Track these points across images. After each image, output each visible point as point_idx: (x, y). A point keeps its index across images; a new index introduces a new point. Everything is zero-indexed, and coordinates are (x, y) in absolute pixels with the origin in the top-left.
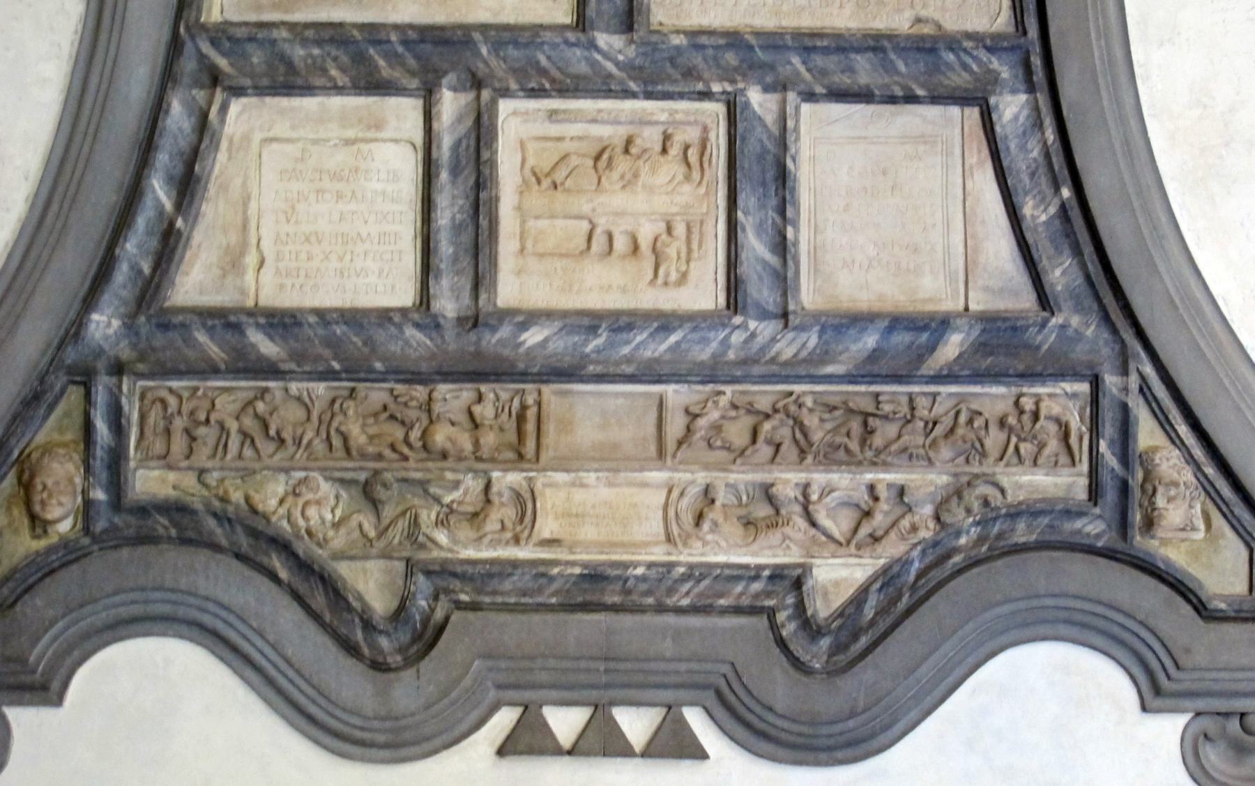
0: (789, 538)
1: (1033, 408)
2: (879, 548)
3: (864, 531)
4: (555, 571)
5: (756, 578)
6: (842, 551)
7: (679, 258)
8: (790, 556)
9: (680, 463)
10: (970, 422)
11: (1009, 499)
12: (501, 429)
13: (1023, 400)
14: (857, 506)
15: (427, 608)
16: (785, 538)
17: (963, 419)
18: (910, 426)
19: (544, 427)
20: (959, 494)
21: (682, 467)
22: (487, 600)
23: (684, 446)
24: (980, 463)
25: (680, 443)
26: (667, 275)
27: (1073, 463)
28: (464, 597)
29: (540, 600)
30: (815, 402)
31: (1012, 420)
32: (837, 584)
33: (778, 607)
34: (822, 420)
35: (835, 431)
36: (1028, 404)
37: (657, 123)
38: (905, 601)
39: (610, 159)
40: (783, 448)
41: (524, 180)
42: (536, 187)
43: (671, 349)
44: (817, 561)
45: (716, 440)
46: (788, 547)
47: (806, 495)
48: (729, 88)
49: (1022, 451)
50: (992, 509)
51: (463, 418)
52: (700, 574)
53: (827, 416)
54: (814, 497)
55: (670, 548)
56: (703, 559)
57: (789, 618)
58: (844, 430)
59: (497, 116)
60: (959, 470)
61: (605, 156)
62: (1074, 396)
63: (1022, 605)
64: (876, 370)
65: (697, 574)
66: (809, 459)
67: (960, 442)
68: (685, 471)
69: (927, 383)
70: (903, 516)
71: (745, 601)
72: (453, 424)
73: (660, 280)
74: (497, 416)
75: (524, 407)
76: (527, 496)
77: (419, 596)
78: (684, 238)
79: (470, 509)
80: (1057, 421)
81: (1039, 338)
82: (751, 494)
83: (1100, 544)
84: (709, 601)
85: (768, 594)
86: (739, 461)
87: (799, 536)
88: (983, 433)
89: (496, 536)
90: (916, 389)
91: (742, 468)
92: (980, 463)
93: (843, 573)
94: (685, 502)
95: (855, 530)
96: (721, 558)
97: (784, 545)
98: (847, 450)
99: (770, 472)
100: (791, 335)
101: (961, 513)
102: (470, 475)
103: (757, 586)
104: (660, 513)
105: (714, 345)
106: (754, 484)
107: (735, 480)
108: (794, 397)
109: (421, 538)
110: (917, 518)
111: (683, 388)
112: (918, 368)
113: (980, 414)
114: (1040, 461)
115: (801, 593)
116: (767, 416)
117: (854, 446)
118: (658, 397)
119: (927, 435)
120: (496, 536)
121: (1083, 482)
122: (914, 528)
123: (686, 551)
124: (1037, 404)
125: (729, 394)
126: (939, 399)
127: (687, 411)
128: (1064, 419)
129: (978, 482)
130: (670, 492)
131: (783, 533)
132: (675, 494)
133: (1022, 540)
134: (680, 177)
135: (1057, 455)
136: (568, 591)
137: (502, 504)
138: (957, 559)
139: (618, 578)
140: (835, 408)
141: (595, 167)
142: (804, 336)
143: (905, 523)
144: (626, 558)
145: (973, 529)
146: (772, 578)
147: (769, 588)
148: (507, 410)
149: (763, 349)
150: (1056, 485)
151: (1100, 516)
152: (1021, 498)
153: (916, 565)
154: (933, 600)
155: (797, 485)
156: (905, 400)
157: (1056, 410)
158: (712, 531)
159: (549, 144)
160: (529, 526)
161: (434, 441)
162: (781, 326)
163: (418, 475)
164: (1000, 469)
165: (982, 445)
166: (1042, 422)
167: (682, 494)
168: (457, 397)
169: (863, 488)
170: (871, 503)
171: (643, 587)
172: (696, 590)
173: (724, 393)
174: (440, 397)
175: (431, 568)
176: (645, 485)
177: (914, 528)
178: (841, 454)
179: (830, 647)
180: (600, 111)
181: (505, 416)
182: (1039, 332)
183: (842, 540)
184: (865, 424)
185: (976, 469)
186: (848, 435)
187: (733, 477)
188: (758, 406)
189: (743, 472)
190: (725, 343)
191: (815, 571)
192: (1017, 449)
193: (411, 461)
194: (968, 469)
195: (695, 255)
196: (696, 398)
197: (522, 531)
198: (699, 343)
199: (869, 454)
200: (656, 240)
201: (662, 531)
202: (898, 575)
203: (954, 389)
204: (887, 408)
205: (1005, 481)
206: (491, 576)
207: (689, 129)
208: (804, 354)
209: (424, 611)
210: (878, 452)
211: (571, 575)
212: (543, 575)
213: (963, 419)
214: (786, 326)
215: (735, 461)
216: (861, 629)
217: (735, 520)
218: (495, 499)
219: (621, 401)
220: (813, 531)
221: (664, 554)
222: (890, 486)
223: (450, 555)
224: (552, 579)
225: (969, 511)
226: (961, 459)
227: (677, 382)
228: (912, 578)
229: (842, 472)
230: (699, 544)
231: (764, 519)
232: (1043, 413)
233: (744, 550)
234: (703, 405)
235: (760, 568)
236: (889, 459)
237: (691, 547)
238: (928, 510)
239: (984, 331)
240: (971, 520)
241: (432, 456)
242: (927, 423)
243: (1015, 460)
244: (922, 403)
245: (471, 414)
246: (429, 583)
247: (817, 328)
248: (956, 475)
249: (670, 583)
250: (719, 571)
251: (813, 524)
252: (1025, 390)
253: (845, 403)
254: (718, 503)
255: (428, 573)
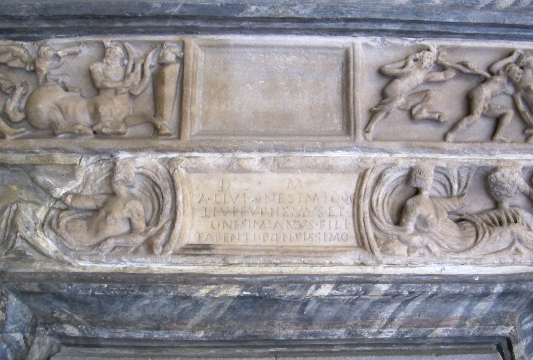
0: (520, 241)
4: (203, 292)
5: (485, 295)
8: (520, 263)
9: (375, 139)
12: (132, 96)
15: (22, 343)
19: (189, 90)
21: (378, 145)
22: (105, 334)
23: (380, 116)
25: (373, 114)
28: (71, 330)
29: (181, 334)
33: (515, 337)
45: (421, 110)
46: (517, 250)
51: (82, 82)
52: (410, 293)
55: (355, 255)
65: (406, 293)
68: (383, 150)
72: (66, 90)
74: (126, 76)
75: (162, 65)
76: (165, 185)
77: (10, 327)
79: (90, 204)
82: (463, 184)
84: (422, 331)
85: (500, 320)
86: (451, 137)
89: (121, 241)
91: (456, 147)
96: (433, 269)
97: (513, 249)
102: (92, 159)
104: (349, 208)
107: (448, 163)
108: (515, 56)
109: (19, 244)
111: (375, 41)
116: (485, 80)
118: (342, 52)
120: (121, 241)
123: (389, 260)
125: (434, 50)
127: (381, 72)
130: (362, 177)
131: (512, 233)
132: (369, 181)
136: (221, 320)
137: (133, 197)
139: (294, 301)
144: (303, 270)
146: (502, 295)
147: (500, 309)
148: (138, 68)
158: (418, 231)
160: (168, 226)
161: (37, 111)
163: (18, 158)
167: (378, 180)
168: (74, 54)
171: (330, 312)
172: (402, 314)
173: (429, 50)
174: (51, 53)
175: (27, 287)
176: (328, 169)
181: (135, 78)
187: (443, 160)
189: (457, 153)
193: (9, 137)
196: (392, 55)
197: (158, 234)
201: (351, 232)
206: (112, 299)
209: (20, 347)
211: (226, 297)
212: (186, 298)
215: (444, 138)
217: (446, 216)
218: (123, 191)
219: (291, 59)
221: (357, 265)
223: (58, 268)
224: (198, 303)
227: (368, 32)
230: (404, 249)
231: (480, 213)
233: (463, 256)
234: (402, 64)
237: (393, 254)
241: (40, 133)
245: (90, 74)
246: (26, 309)
249: (366, 306)
250: (435, 288)
254: (425, 194)
255: (23, 295)
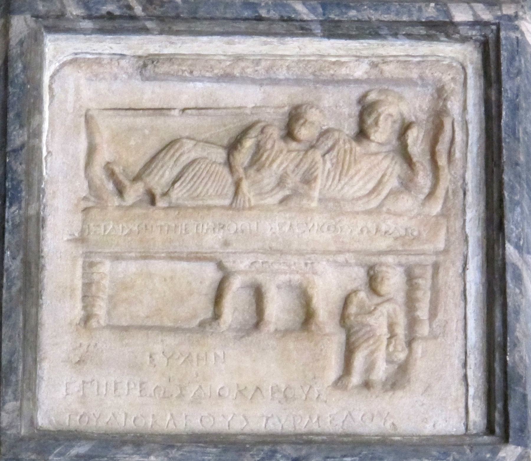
7: (392, 335)
26: (370, 368)
37: (346, 81)
39: (258, 149)
41: (90, 186)
42: (116, 201)
48: (486, 16)
59: (40, 68)
61: (249, 143)
73: (356, 379)
78: (400, 297)
134: (393, 183)
141: (229, 164)
159: (142, 121)
180: (238, 58)
195: (424, 330)
200: (346, 301)
207: (408, 93)
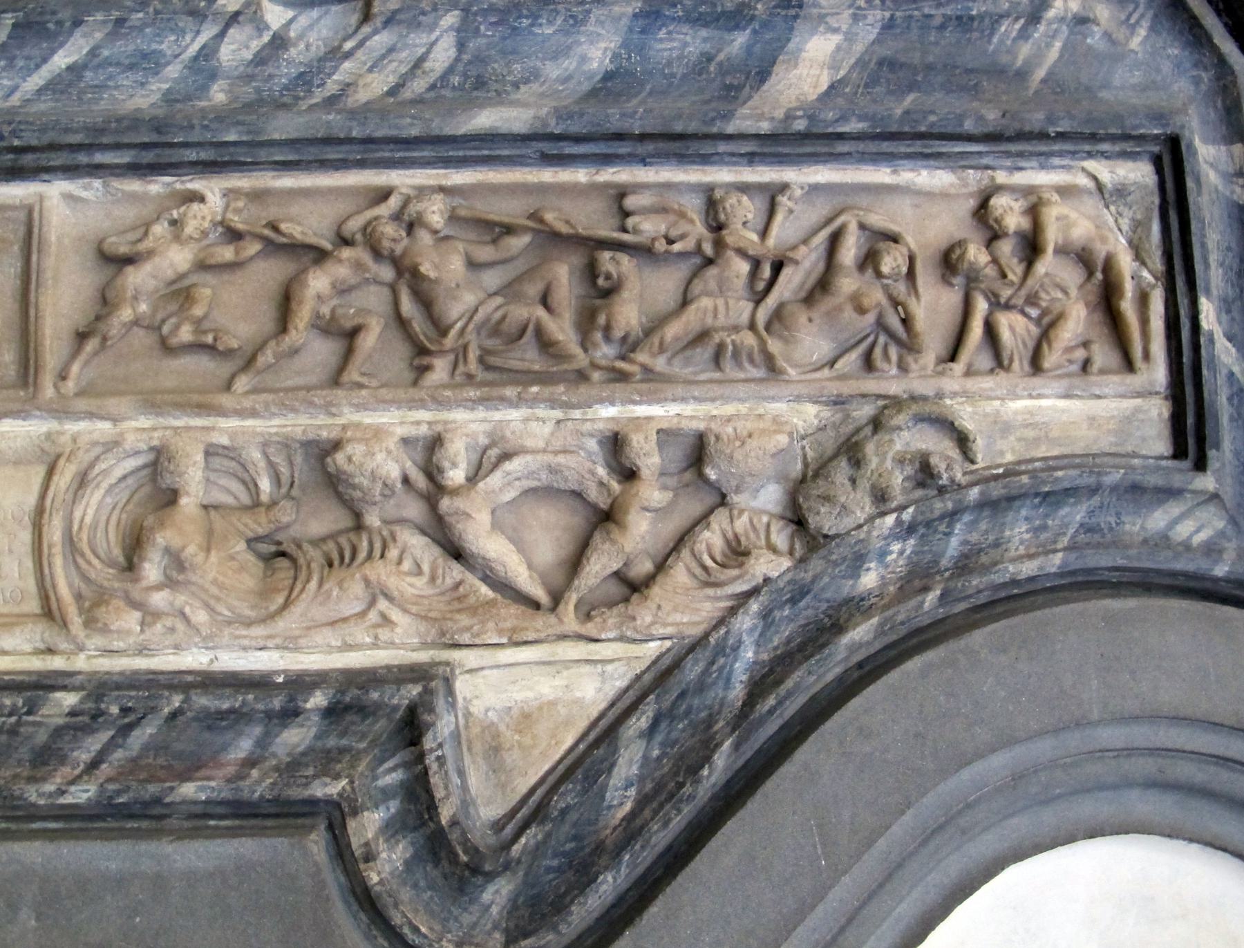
0: (389, 597)
1: (1025, 223)
2: (644, 614)
3: (599, 565)
5: (290, 714)
6: (541, 623)
8: (391, 644)
9: (80, 394)
10: (869, 260)
11: (981, 461)
13: (999, 203)
14: (578, 495)
16: (376, 593)
17: (849, 252)
18: (712, 272)
20: (851, 450)
21: (82, 404)
23: (91, 345)
24: (903, 368)
27: (1129, 365)
30: (453, 218)
31: (976, 254)
32: (526, 719)
33: (352, 801)
34: (473, 265)
35: (510, 290)
36: (1014, 220)
38: (722, 764)
40: (368, 341)
43: (53, 86)
44: (469, 658)
45: (177, 327)
46: (386, 620)
47: (432, 472)
49: (1005, 335)
50: (942, 491)
52: (125, 711)
53: (485, 253)
54: (456, 475)
56: (141, 663)
57: (392, 829)
58: (533, 289)
60: (847, 388)
62: (1121, 192)
63: (1044, 748)
64: (614, 118)
65: (115, 710)
66: (440, 369)
67: (849, 313)
68: (91, 415)
69: (751, 159)
70: (703, 520)
71: (259, 785)
80: (1083, 258)
81: (1025, 50)
82: (285, 479)
83: (1220, 571)
84: (153, 789)
86: (242, 383)
87: (413, 587)
88: (901, 288)
90: (722, 175)
91: (247, 403)
92: (903, 368)
93: (546, 687)
94: (92, 505)
95: (575, 563)
96: (194, 659)
97: (373, 616)
98: (545, 344)
99: (328, 408)
100: (382, 40)
101: (862, 507)
103: (295, 737)
104: (26, 536)
105: (173, 71)
106: (286, 445)
107: (233, 435)
108: (394, 202)
110: (741, 524)
111: (90, 189)
112: (727, 116)
113: (894, 239)
114: (1051, 359)
115: (421, 757)
116: (320, 256)
117: (563, 330)
118: (22, 215)
119: (759, 299)
121: (1158, 410)
122: (738, 553)
123: (95, 642)
124: (1034, 212)
125: (215, 201)
126: (783, 200)
128: (1101, 251)
129: (900, 419)
131: (367, 582)
132: (64, 479)
133: (1028, 568)
135: (1086, 344)
138: (861, 634)
140: (509, 230)
142: (419, 40)
143: (712, 538)
145: (896, 547)
146: (332, 712)
147: (332, 742)
149: (306, 79)
150: (1092, 419)
151: (1215, 497)
152: (1009, 458)
153: (749, 654)
154: (804, 754)
155: (405, 441)
156: (693, 205)
157: (1081, 230)
158: (169, 583)
162: (354, 19)
164: (953, 380)
165: (906, 322)
166: (1044, 266)
167: (82, 481)
169: (592, 444)
170: (616, 486)
172: (119, 754)
173: (202, 199)
177: (738, 553)
178: (528, 356)
179: (513, 906)
182: (1023, 35)
183: (539, 593)
184: (591, 271)
185: (894, 387)
186: (545, 301)
187: (225, 428)
188: (294, 230)
189: (253, 414)
190: (205, 60)
191: (462, 686)
192: (991, 332)
194: (871, 385)
196: (129, 214)
198: (131, 67)
199: (605, 352)
201: (31, 585)
202: (701, 686)
203: (823, 174)
204: (649, 227)
205: (966, 416)
208: (418, 86)
210: (629, 347)
213: (849, 252)
214: (366, 17)
215: (228, 386)
216: (599, 848)
217: (242, 546)
220: (456, 571)
221: (38, 652)
222: (666, 436)
225: (880, 497)
226: (852, 359)
227: (71, 171)
228: (737, 692)
229: (534, 401)
230: (132, 619)
231: (318, 542)
232: (1052, 236)
233: (258, 631)
234: (138, 234)
235: (300, 683)
236: (660, 364)
237: (105, 630)
238: (770, 497)
239: (889, 26)
240: (890, 520)
242: (756, 264)
243: (985, 361)
244: (745, 211)
247: (451, 19)
248: (838, 402)
249: (42, 737)
250: (177, 700)
251: (457, 553)
252: (1001, 177)
253: (535, 216)
254: (188, 503)
